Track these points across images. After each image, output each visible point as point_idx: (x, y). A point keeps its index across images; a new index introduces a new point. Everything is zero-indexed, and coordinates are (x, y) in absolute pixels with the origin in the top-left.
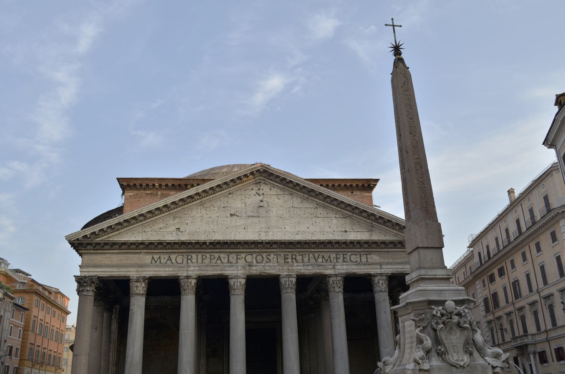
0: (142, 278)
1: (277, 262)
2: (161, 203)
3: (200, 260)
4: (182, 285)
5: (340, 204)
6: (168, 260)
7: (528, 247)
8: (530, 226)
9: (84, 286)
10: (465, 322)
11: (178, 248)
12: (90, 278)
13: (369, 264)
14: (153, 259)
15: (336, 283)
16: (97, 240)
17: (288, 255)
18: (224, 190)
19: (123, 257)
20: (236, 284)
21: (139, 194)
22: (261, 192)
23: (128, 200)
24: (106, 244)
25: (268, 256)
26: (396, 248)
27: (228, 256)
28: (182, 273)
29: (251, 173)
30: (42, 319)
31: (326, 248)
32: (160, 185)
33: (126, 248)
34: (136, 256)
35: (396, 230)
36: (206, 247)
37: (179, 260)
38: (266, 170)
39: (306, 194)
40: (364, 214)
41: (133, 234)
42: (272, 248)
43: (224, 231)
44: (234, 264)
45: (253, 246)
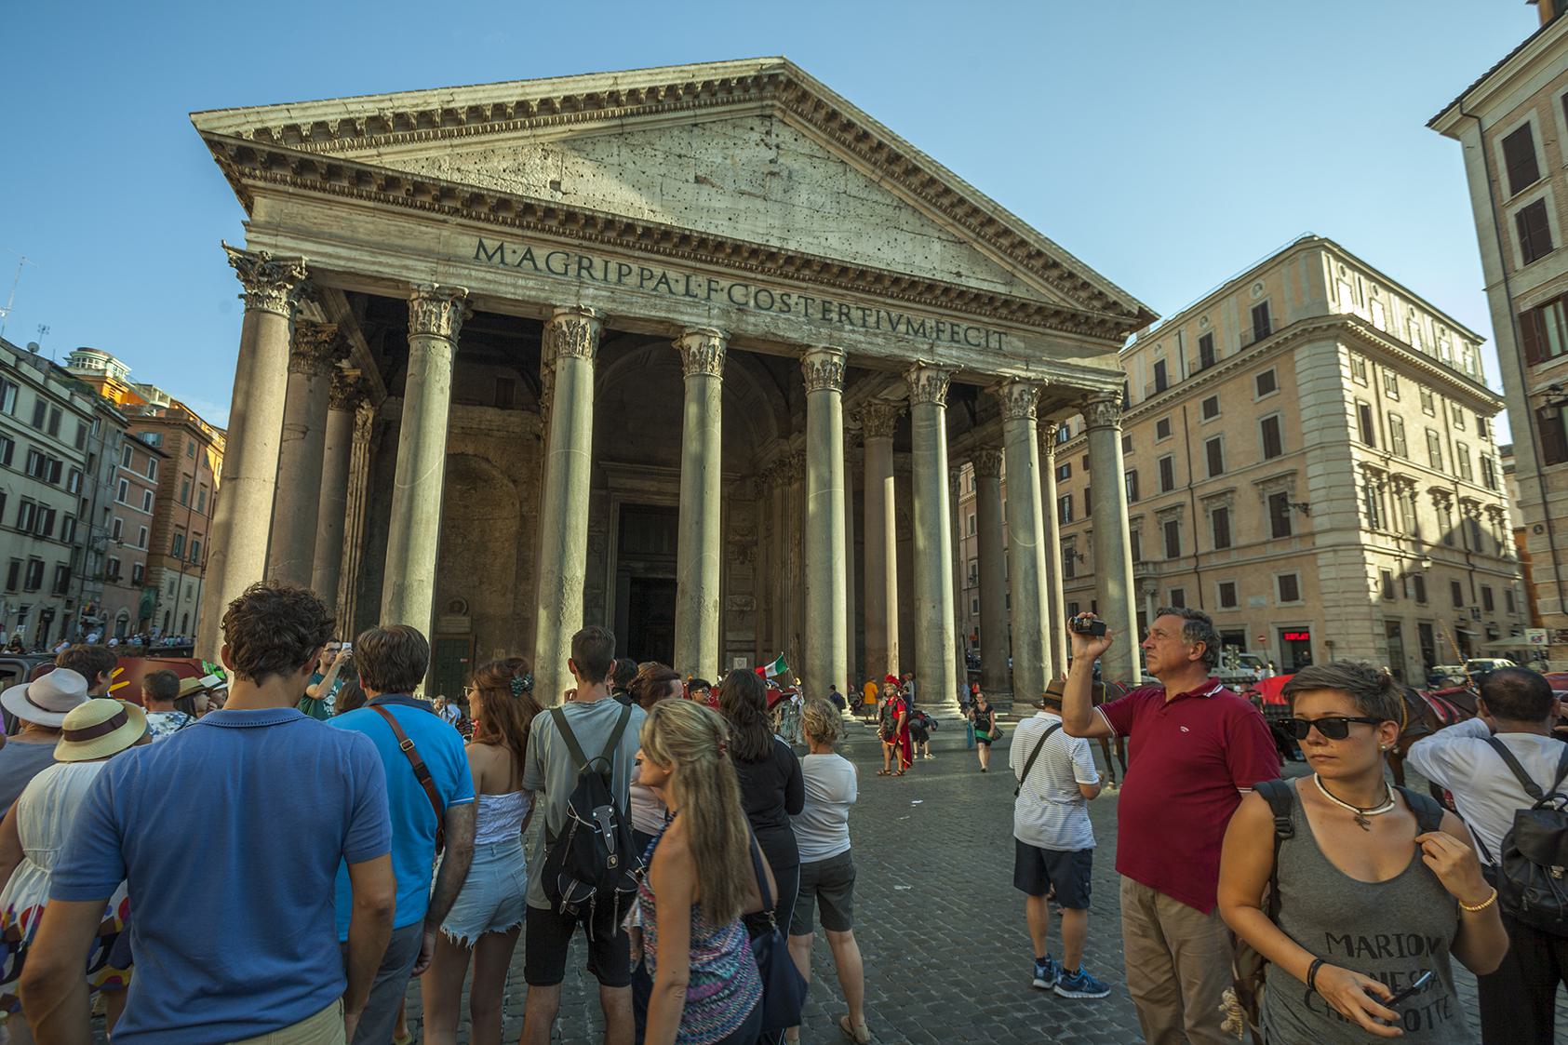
0: (447, 292)
1: (806, 315)
2: (510, 92)
3: (613, 276)
6: (524, 258)
7: (1179, 410)
8: (1196, 370)
12: (282, 263)
13: (1005, 356)
17: (830, 303)
18: (682, 109)
22: (773, 140)
25: (785, 297)
26: (1061, 330)
27: (688, 277)
29: (756, 79)
30: (205, 483)
31: (919, 302)
34: (429, 229)
35: (1062, 290)
38: (795, 80)
40: (1005, 242)
42: (798, 279)
45: (753, 262)
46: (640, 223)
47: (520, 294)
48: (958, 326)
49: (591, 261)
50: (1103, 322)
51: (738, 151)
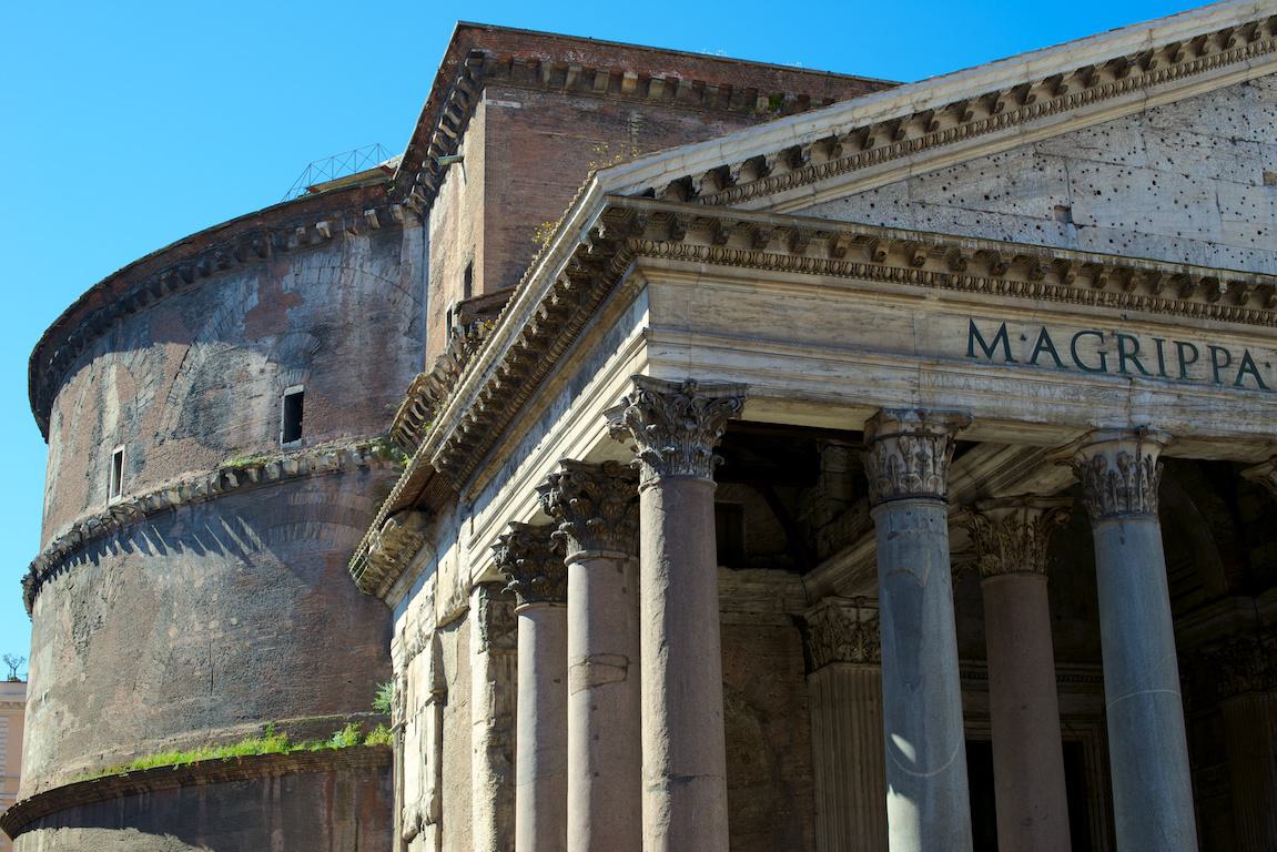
0: (942, 419)
3: (1172, 367)
4: (1112, 475)
6: (1039, 348)
11: (1087, 293)
14: (975, 339)
19: (838, 310)
21: (547, 109)
23: (501, 129)
28: (1109, 414)
32: (645, 81)
33: (863, 269)
34: (896, 312)
36: (1205, 306)
37: (1089, 357)
41: (874, 211)
43: (1251, 245)
46: (1227, 276)
47: (1043, 412)
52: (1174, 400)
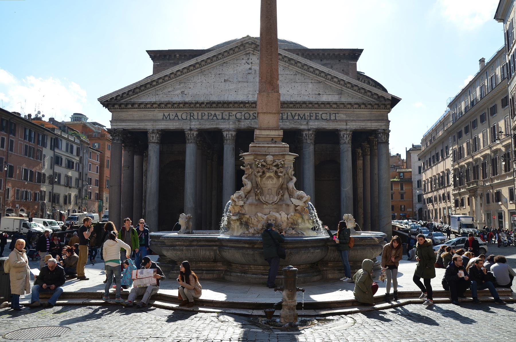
3: (200, 117)
5: (314, 71)
6: (175, 116)
9: (114, 136)
10: (281, 172)
15: (309, 136)
16: (121, 101)
18: (219, 60)
20: (228, 135)
21: (164, 63)
22: (250, 61)
24: (126, 105)
25: (254, 114)
26: (361, 109)
27: (222, 113)
28: (186, 127)
29: (241, 45)
31: (302, 108)
35: (361, 93)
36: (205, 107)
37: (184, 117)
39: (288, 63)
44: (227, 120)
45: (242, 105)
46: (205, 102)
48: (318, 113)
49: (193, 114)
50: (376, 104)
51: (238, 68)
52: (199, 123)
